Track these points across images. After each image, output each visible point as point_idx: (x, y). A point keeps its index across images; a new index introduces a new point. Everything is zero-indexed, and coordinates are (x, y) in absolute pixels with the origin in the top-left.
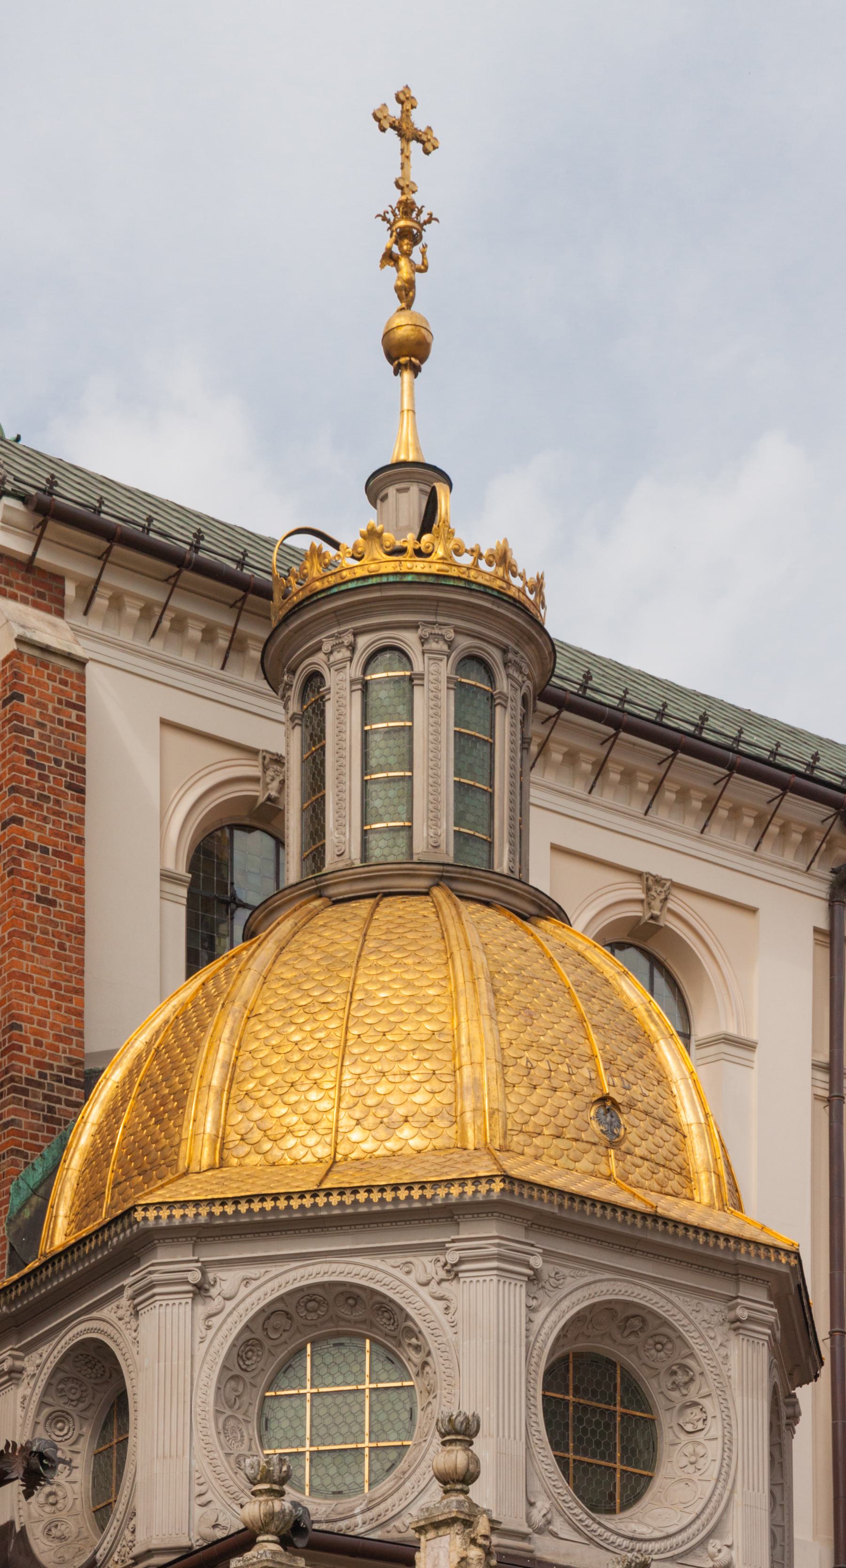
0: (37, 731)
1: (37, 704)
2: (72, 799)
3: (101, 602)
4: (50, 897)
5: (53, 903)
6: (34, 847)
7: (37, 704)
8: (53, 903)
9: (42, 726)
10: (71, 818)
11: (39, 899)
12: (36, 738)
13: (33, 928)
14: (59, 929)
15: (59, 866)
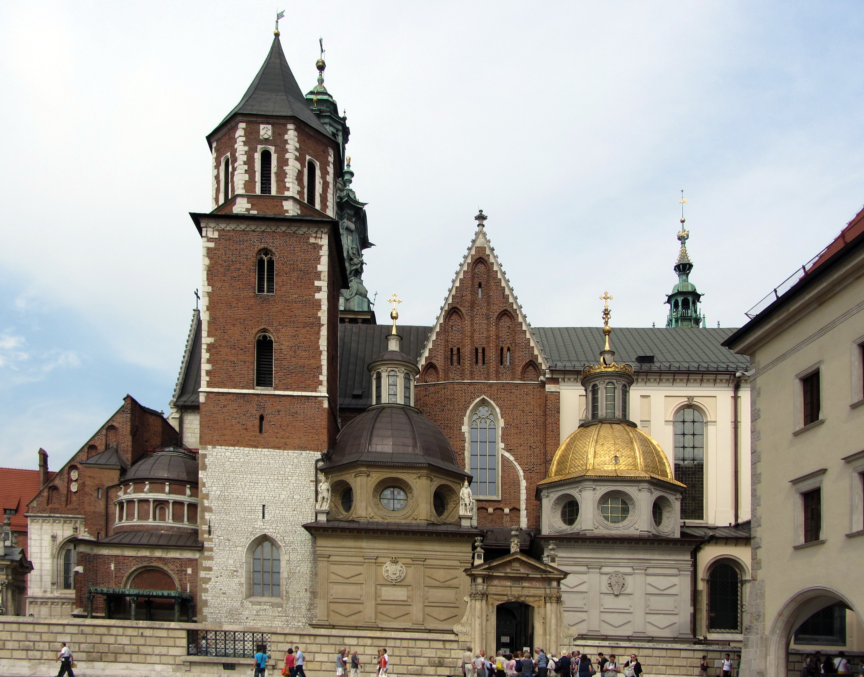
15: (555, 425)
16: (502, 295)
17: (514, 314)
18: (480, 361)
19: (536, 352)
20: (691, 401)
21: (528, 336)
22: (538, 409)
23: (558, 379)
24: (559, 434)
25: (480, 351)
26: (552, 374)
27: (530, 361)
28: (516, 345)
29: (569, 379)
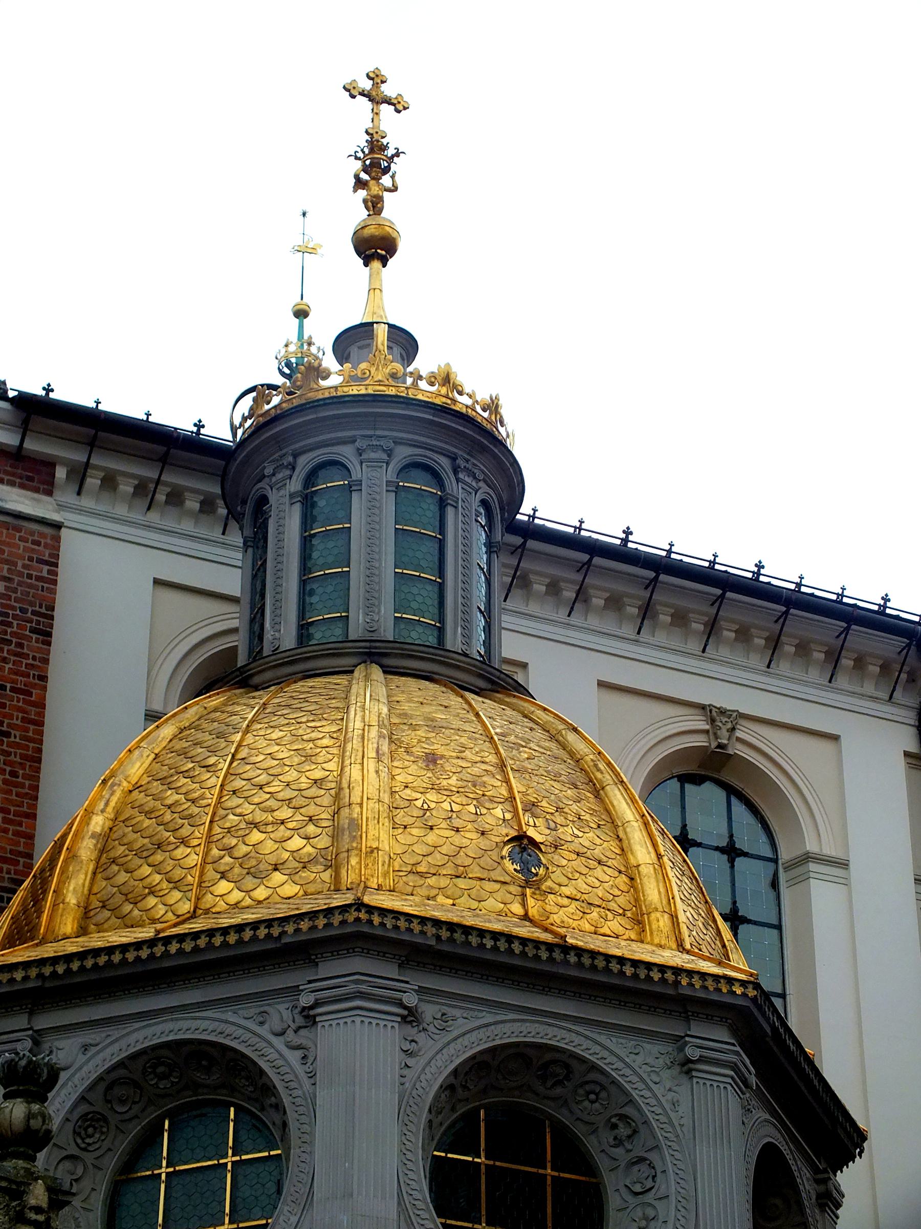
2: (37, 641)
3: (93, 482)
10: (34, 658)
14: (12, 757)
15: (18, 701)
20: (724, 733)
23: (49, 465)
24: (35, 759)
26: (25, 429)
29: (109, 482)
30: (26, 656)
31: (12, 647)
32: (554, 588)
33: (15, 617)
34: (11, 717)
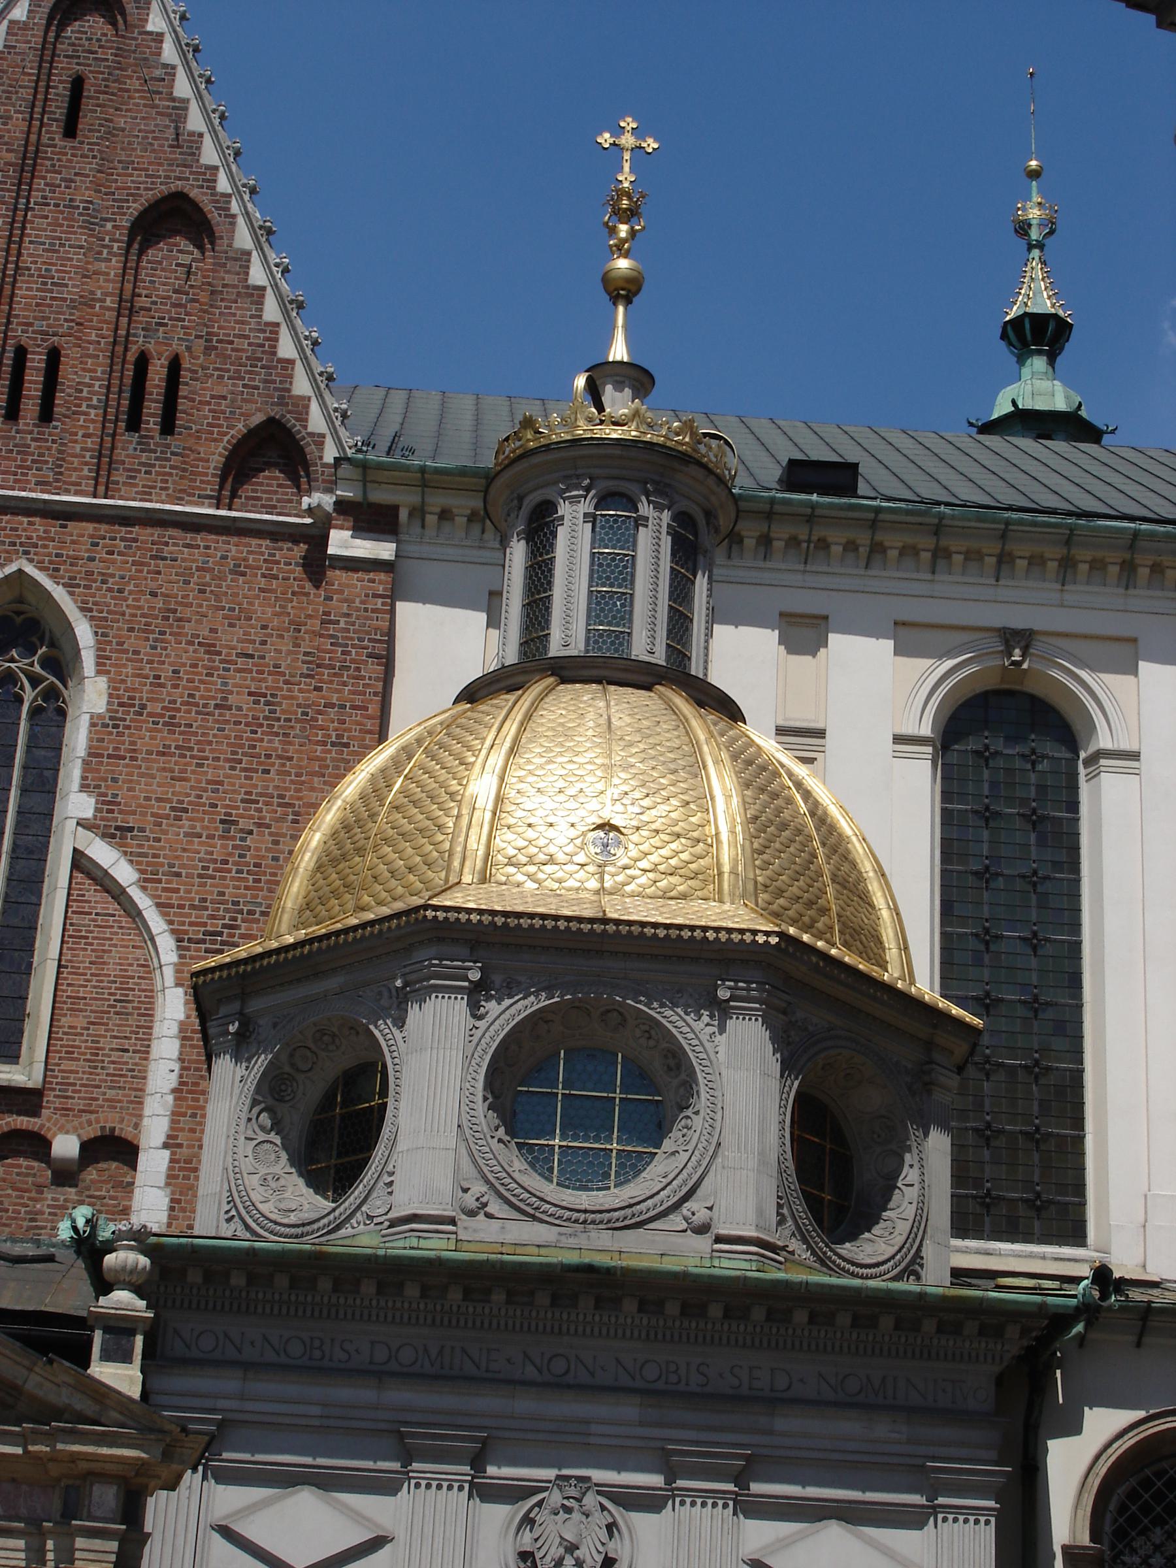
0: (342, 620)
1: (346, 601)
2: (373, 664)
3: (431, 519)
4: (345, 740)
5: (347, 745)
6: (333, 706)
7: (346, 601)
8: (347, 745)
9: (348, 615)
10: (370, 678)
11: (333, 744)
12: (342, 625)
13: (327, 767)
16: (170, 133)
17: (215, 217)
18: (30, 406)
19: (301, 386)
21: (271, 311)
22: (286, 646)
23: (394, 509)
25: (36, 361)
27: (271, 421)
28: (208, 349)
30: (363, 678)
31: (351, 672)
32: (851, 547)
33: (353, 646)
34: (350, 730)
